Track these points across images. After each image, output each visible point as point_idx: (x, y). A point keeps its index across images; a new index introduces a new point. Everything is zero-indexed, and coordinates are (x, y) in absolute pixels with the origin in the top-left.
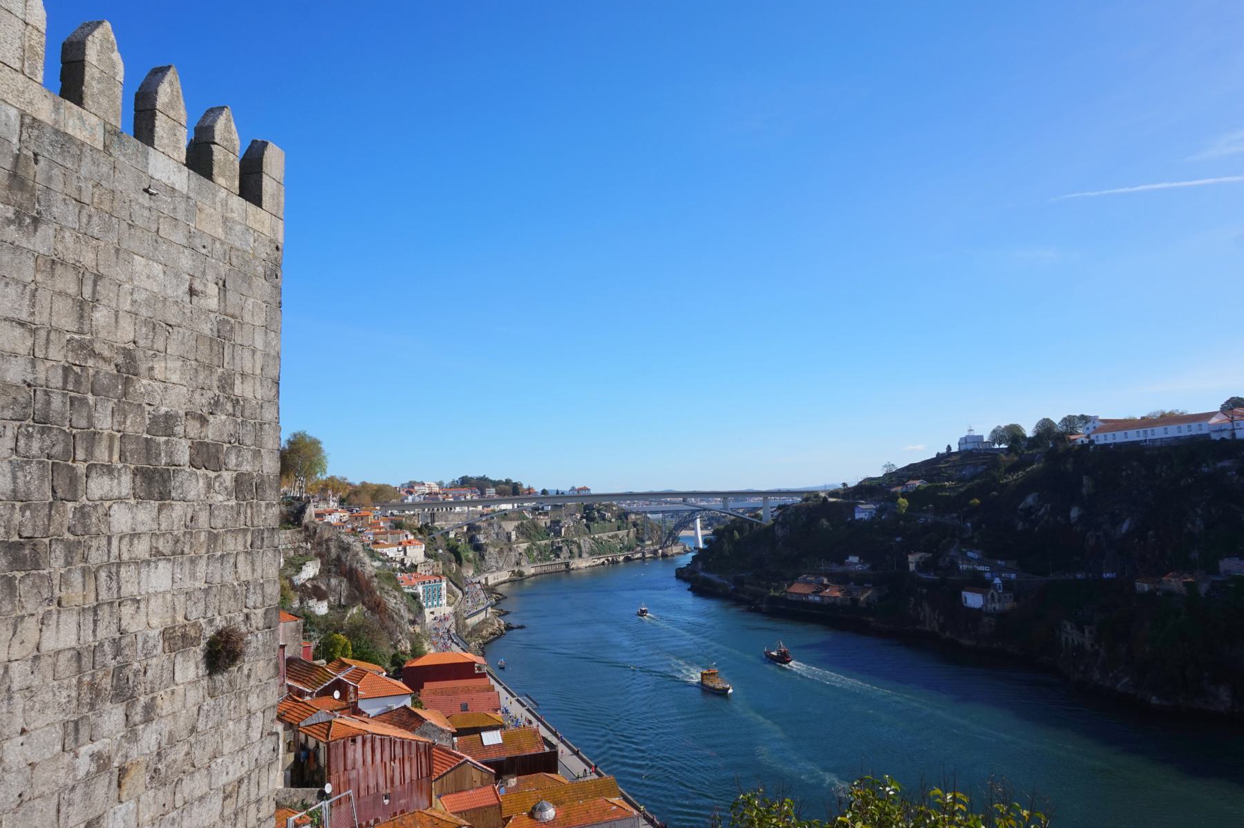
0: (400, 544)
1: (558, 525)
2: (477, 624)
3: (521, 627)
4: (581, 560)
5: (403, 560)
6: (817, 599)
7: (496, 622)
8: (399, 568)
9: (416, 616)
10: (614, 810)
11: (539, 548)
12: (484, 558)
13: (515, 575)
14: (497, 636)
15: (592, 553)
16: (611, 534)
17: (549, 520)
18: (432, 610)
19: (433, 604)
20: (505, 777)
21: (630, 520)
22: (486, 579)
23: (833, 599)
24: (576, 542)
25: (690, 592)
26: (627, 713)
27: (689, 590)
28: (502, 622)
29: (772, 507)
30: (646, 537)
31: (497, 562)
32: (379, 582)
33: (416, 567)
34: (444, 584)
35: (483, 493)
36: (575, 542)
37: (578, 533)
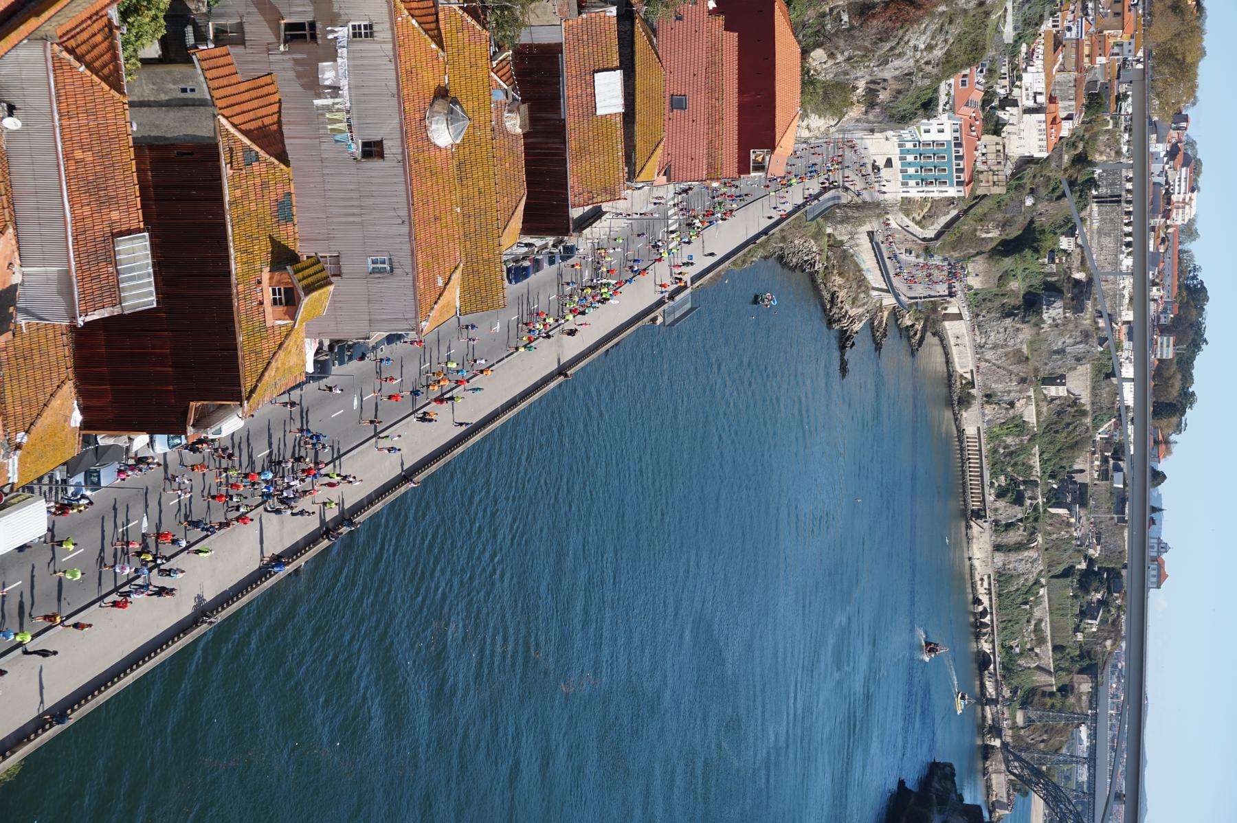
0: (1052, 100)
1: (1074, 501)
2: (857, 265)
3: (844, 370)
4: (989, 548)
5: (1015, 103)
7: (860, 310)
8: (995, 93)
9: (885, 108)
10: (435, 280)
11: (1023, 449)
12: (1008, 315)
13: (964, 387)
14: (828, 312)
15: (1003, 577)
16: (1046, 627)
17: (1088, 481)
18: (897, 163)
19: (910, 164)
20: (524, 108)
21: (1077, 678)
22: (959, 317)
24: (1030, 541)
25: (893, 786)
27: (901, 783)
28: (857, 327)
30: (1033, 714)
31: (995, 347)
32: (965, 11)
33: (997, 132)
34: (952, 192)
35: (1164, 330)
36: (1031, 537)
37: (1054, 546)
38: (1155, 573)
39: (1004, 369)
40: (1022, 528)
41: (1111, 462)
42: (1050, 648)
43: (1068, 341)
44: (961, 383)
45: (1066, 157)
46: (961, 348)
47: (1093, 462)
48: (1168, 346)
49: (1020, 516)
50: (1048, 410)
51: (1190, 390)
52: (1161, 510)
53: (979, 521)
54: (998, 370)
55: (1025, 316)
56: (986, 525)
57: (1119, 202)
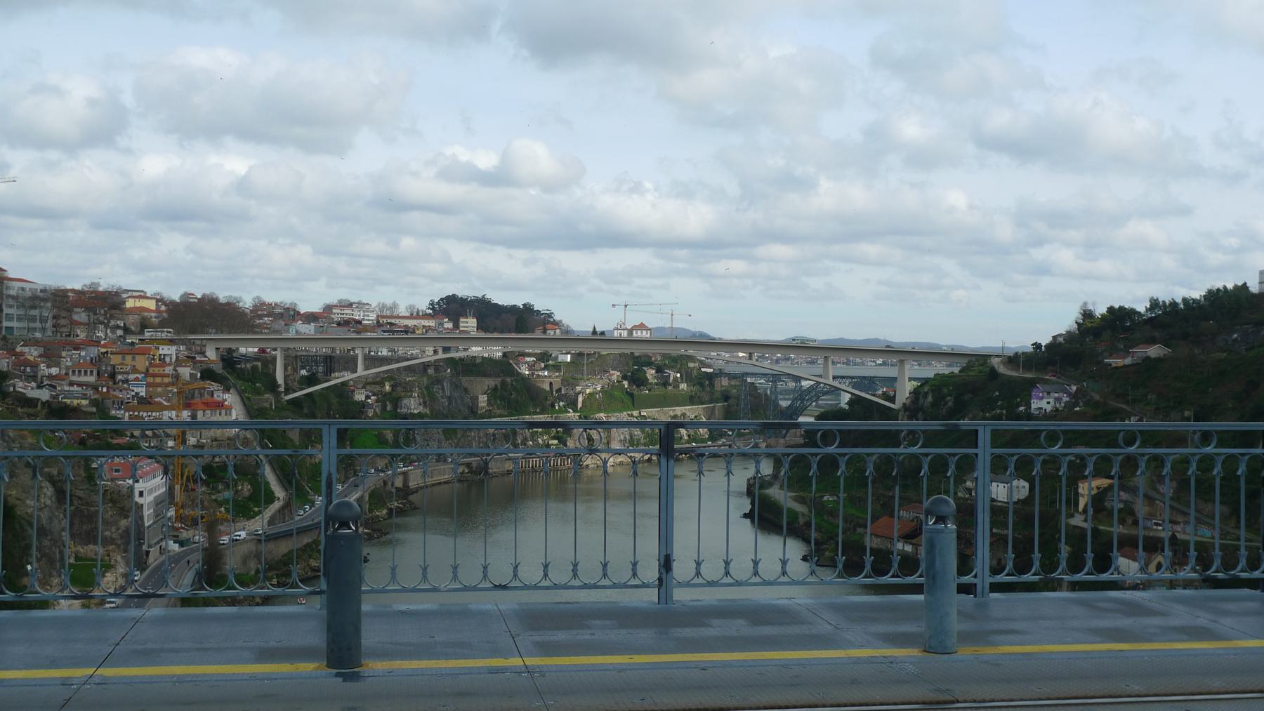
6: (908, 548)
29: (911, 379)
35: (456, 326)
38: (639, 332)
43: (441, 394)
47: (546, 376)
48: (467, 322)
51: (522, 307)
52: (594, 328)
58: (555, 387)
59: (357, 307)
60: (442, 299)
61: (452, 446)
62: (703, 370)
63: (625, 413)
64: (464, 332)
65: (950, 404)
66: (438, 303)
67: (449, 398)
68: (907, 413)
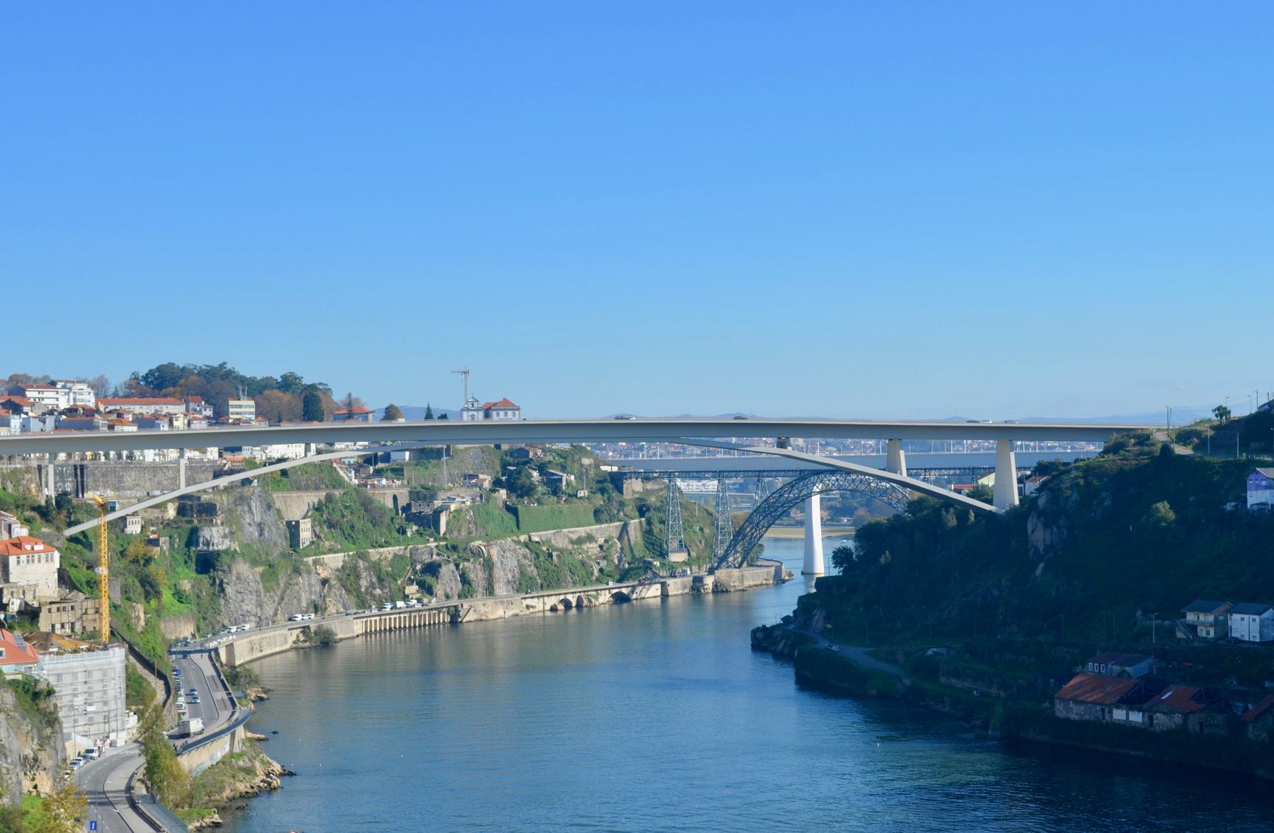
4: (490, 602)
6: (1136, 717)
7: (257, 764)
11: (375, 567)
12: (223, 590)
15: (523, 585)
17: (405, 491)
22: (230, 647)
23: (1178, 718)
26: (600, 819)
30: (674, 544)
36: (477, 553)
38: (502, 413)
39: (284, 592)
40: (466, 564)
41: (380, 465)
42: (598, 526)
44: (305, 641)
45: (44, 530)
46: (264, 643)
47: (384, 486)
48: (240, 406)
49: (452, 567)
50: (328, 540)
51: (280, 380)
52: (429, 409)
53: (461, 614)
54: (286, 599)
55: (223, 571)
56: (466, 606)
57: (82, 468)
58: (403, 502)
59: (64, 387)
60: (151, 372)
61: (274, 601)
62: (604, 468)
63: (509, 539)
64: (237, 422)
65: (1108, 503)
66: (145, 378)
67: (259, 525)
68: (1042, 519)
